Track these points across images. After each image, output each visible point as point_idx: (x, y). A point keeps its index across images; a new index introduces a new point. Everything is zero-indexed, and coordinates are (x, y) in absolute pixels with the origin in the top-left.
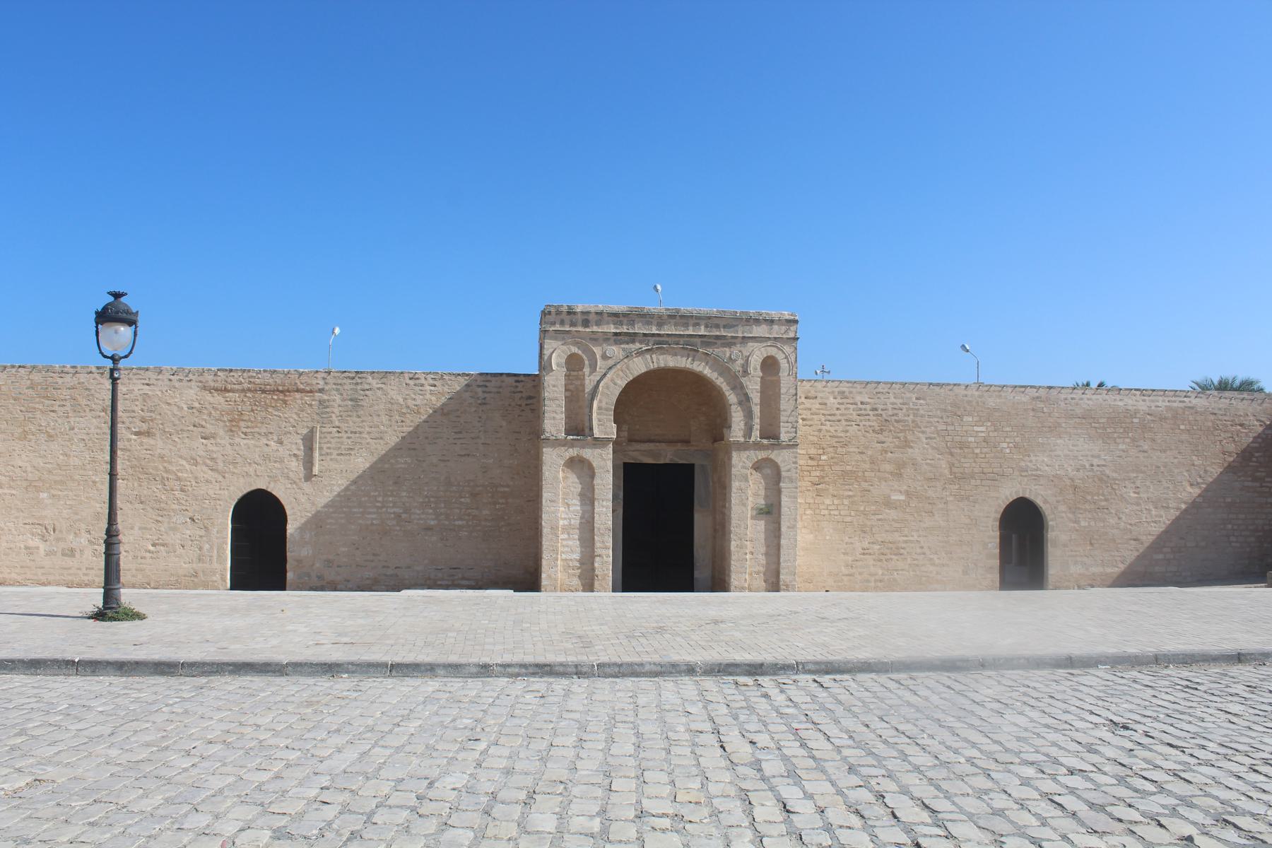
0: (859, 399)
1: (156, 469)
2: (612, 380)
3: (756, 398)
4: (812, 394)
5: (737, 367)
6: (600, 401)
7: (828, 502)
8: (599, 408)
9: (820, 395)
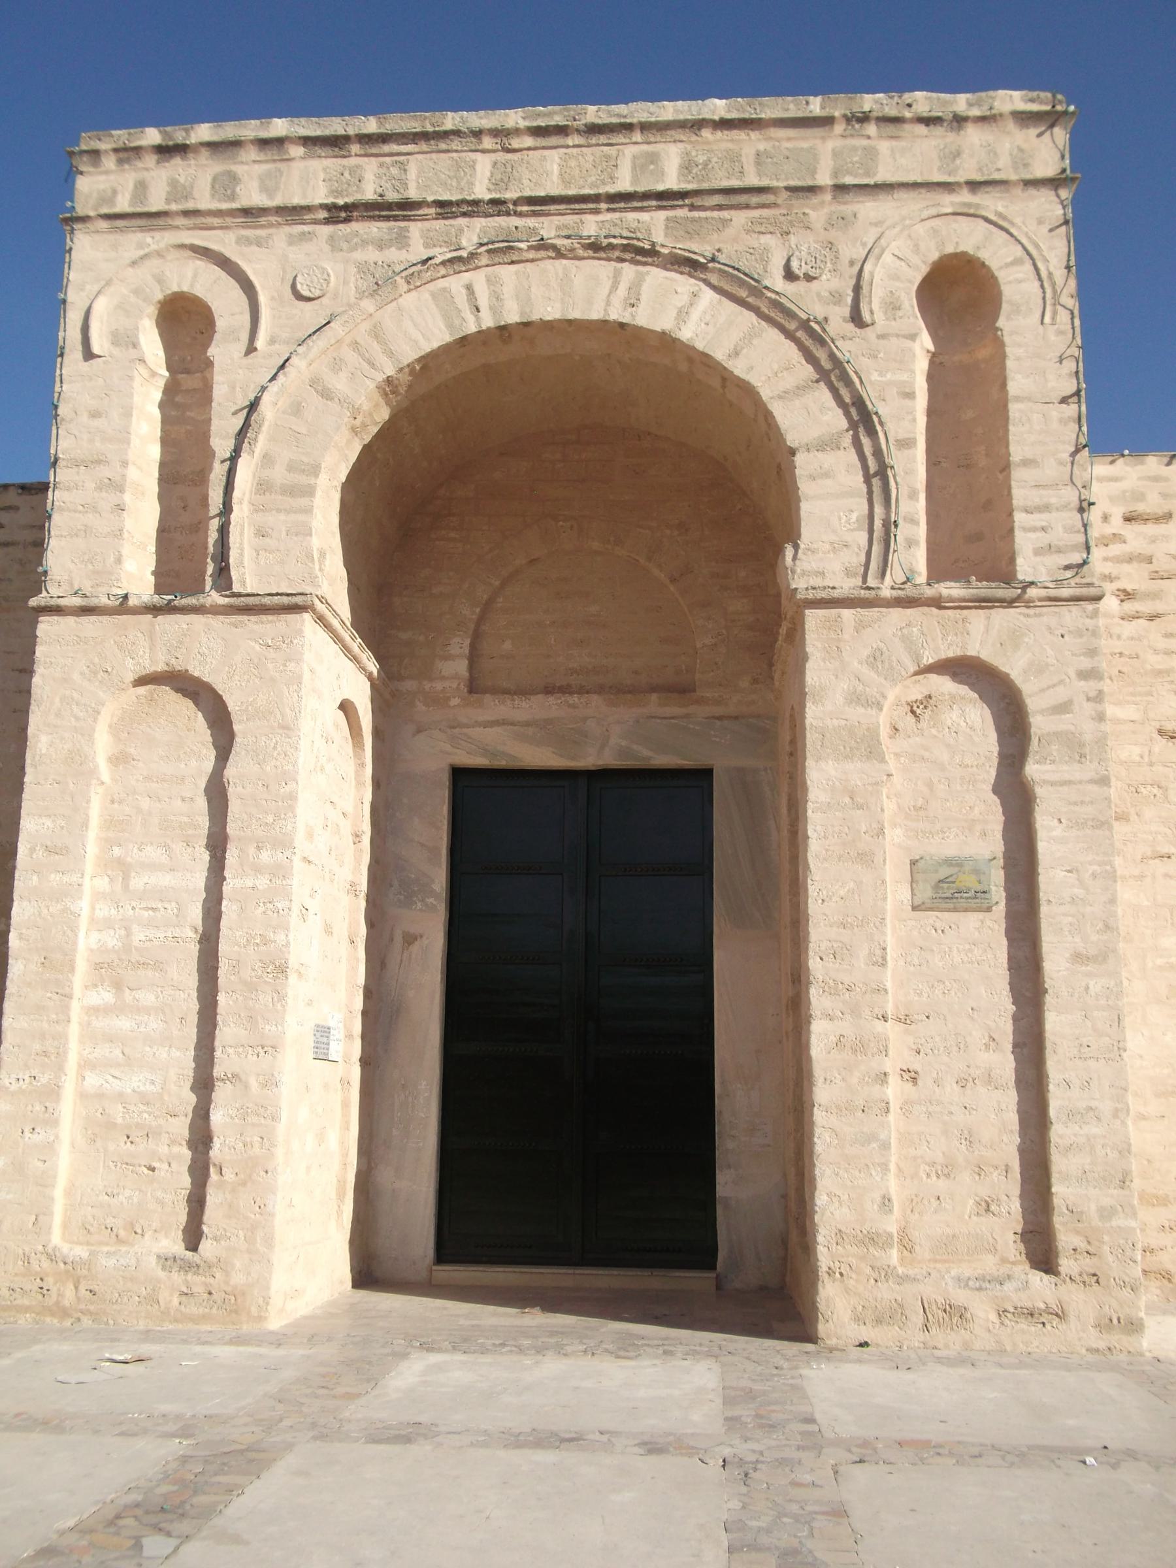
3: (907, 418)
4: (1152, 504)
5: (817, 299)
6: (268, 460)
8: (262, 486)
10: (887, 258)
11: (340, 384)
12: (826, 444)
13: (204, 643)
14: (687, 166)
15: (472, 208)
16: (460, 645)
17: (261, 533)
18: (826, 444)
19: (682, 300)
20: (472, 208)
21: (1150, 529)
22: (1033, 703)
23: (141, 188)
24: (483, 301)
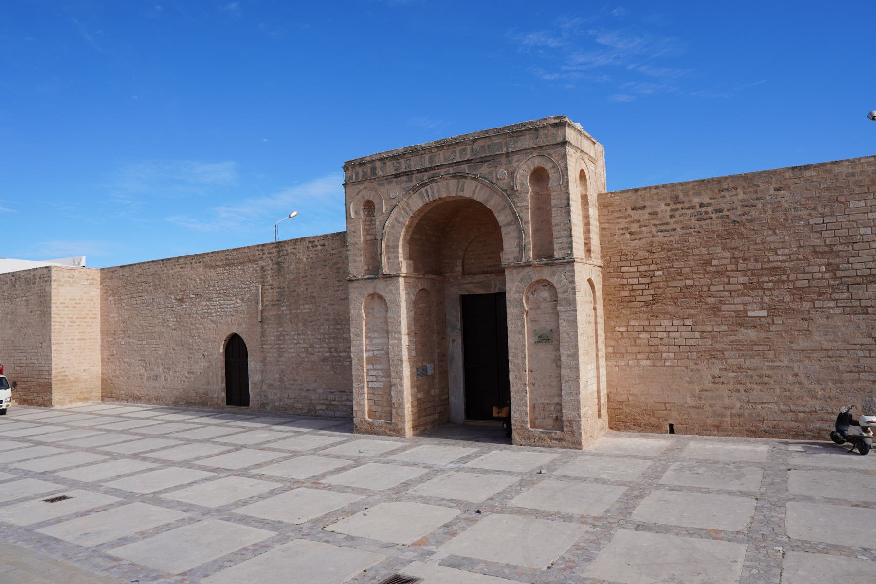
0: (696, 201)
1: (187, 322)
2: (396, 219)
4: (641, 203)
7: (666, 322)
8: (388, 247)
9: (647, 204)
10: (521, 171)
11: (401, 220)
12: (509, 224)
13: (380, 287)
14: (472, 151)
15: (426, 170)
16: (459, 262)
17: (389, 259)
18: (509, 224)
19: (474, 188)
20: (426, 170)
21: (639, 212)
22: (559, 291)
23: (357, 174)
24: (430, 194)
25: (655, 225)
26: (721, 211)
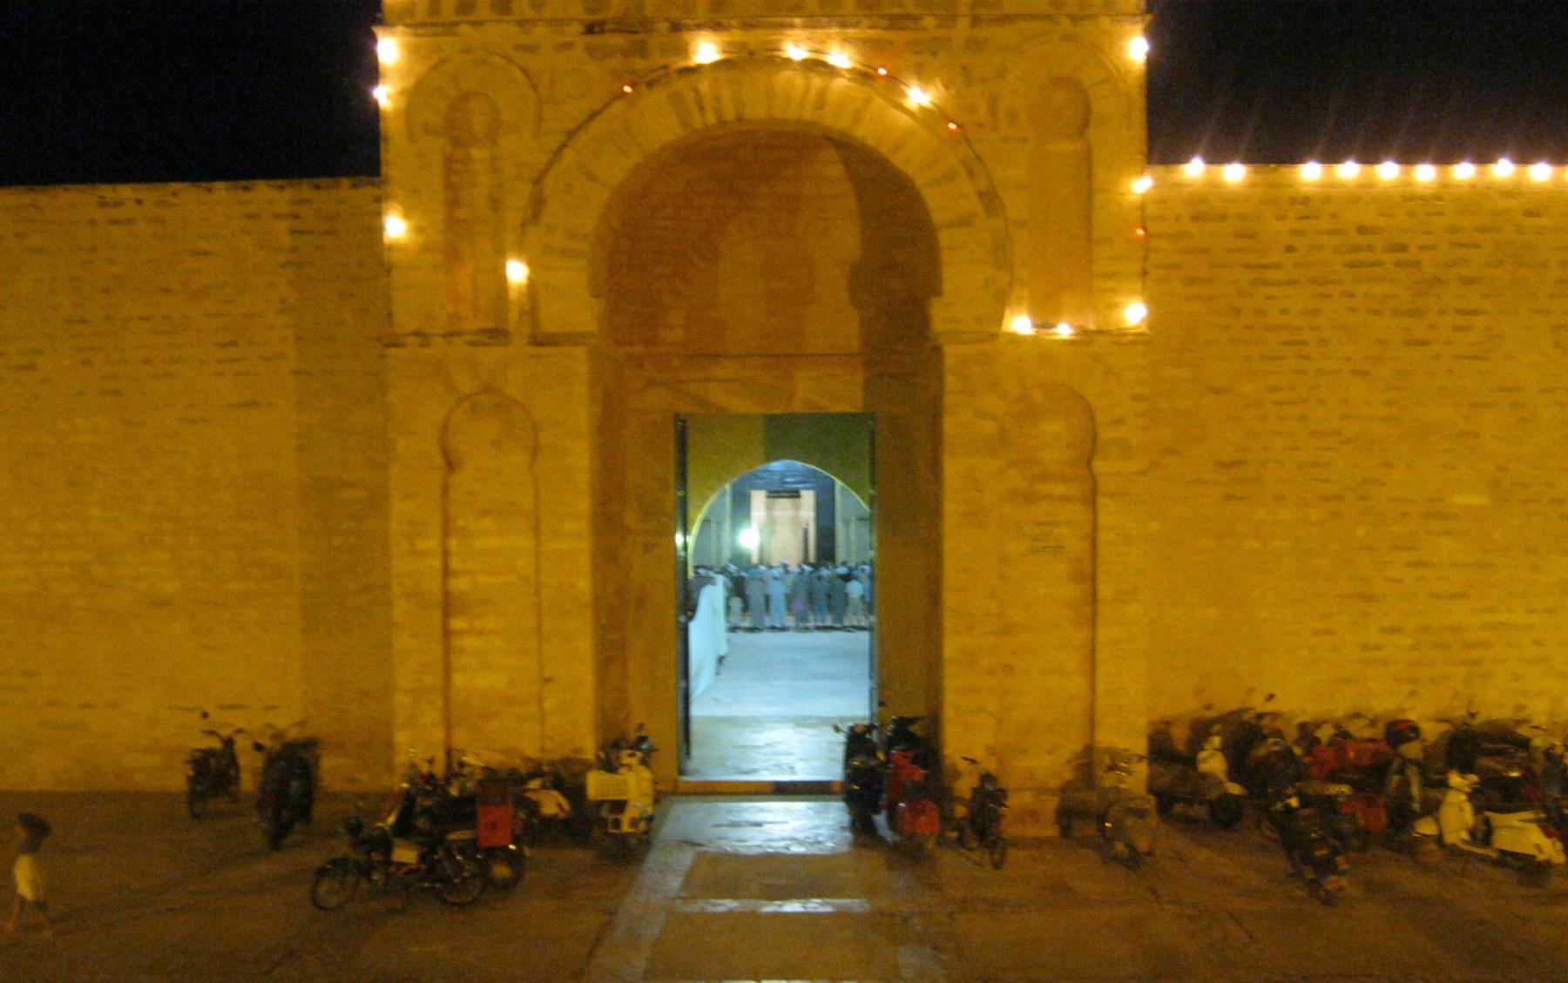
12: (965, 222)
18: (965, 222)
25: (1247, 266)
26: (1403, 248)
